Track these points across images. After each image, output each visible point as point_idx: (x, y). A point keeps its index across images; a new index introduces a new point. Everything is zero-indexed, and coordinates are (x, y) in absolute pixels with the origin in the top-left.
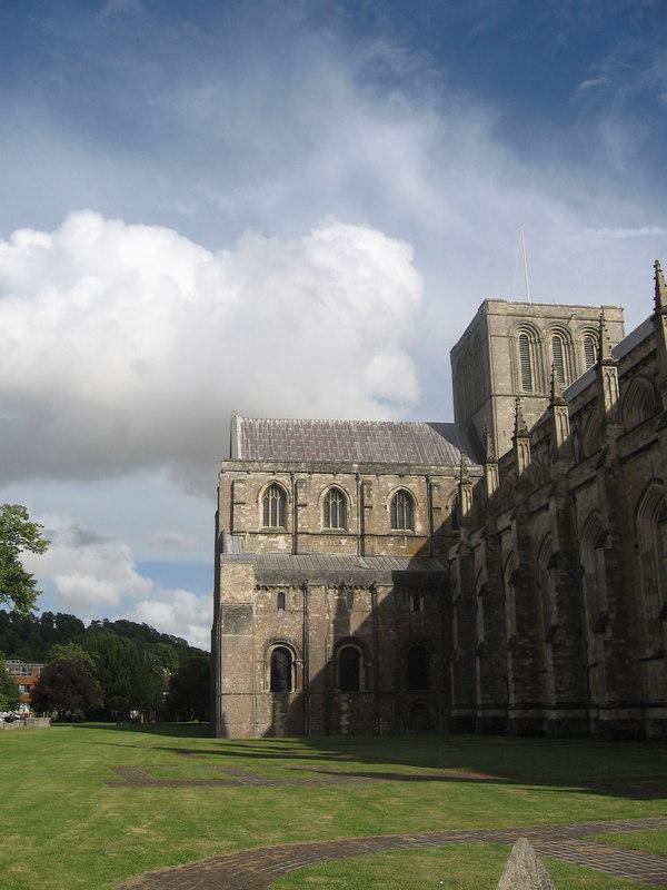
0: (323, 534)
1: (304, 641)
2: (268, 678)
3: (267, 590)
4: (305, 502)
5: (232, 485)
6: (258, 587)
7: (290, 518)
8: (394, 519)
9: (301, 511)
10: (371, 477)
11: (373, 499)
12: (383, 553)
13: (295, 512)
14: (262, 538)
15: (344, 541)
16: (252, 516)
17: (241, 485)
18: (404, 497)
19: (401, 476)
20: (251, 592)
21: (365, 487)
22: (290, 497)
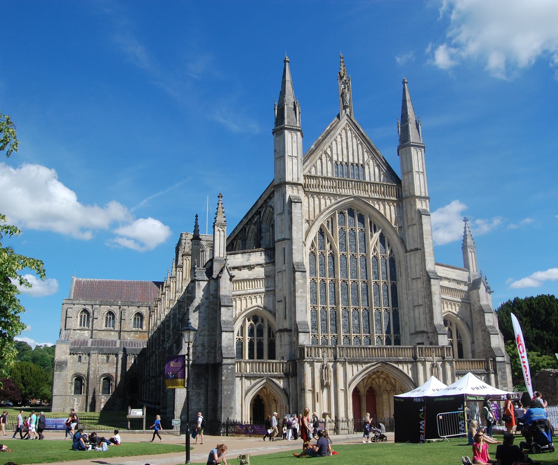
0: (104, 330)
1: (88, 375)
2: (73, 389)
3: (74, 355)
4: (97, 317)
5: (67, 311)
6: (71, 354)
7: (91, 324)
8: (135, 324)
9: (95, 321)
10: (125, 307)
11: (126, 316)
12: (129, 338)
13: (93, 321)
14: (78, 331)
15: (112, 333)
16: (75, 322)
17: (71, 310)
18: (139, 315)
19: (139, 307)
20: (68, 355)
21: (123, 311)
22: (91, 315)
